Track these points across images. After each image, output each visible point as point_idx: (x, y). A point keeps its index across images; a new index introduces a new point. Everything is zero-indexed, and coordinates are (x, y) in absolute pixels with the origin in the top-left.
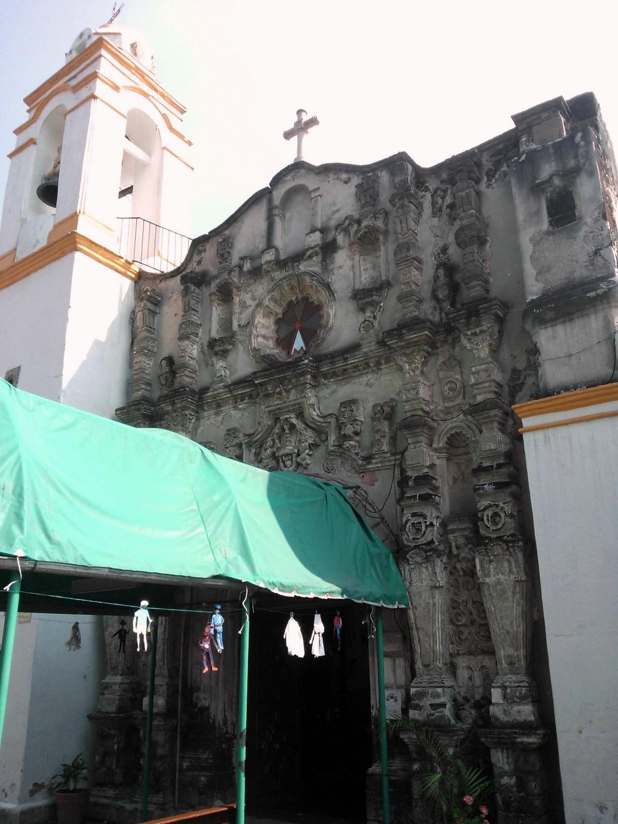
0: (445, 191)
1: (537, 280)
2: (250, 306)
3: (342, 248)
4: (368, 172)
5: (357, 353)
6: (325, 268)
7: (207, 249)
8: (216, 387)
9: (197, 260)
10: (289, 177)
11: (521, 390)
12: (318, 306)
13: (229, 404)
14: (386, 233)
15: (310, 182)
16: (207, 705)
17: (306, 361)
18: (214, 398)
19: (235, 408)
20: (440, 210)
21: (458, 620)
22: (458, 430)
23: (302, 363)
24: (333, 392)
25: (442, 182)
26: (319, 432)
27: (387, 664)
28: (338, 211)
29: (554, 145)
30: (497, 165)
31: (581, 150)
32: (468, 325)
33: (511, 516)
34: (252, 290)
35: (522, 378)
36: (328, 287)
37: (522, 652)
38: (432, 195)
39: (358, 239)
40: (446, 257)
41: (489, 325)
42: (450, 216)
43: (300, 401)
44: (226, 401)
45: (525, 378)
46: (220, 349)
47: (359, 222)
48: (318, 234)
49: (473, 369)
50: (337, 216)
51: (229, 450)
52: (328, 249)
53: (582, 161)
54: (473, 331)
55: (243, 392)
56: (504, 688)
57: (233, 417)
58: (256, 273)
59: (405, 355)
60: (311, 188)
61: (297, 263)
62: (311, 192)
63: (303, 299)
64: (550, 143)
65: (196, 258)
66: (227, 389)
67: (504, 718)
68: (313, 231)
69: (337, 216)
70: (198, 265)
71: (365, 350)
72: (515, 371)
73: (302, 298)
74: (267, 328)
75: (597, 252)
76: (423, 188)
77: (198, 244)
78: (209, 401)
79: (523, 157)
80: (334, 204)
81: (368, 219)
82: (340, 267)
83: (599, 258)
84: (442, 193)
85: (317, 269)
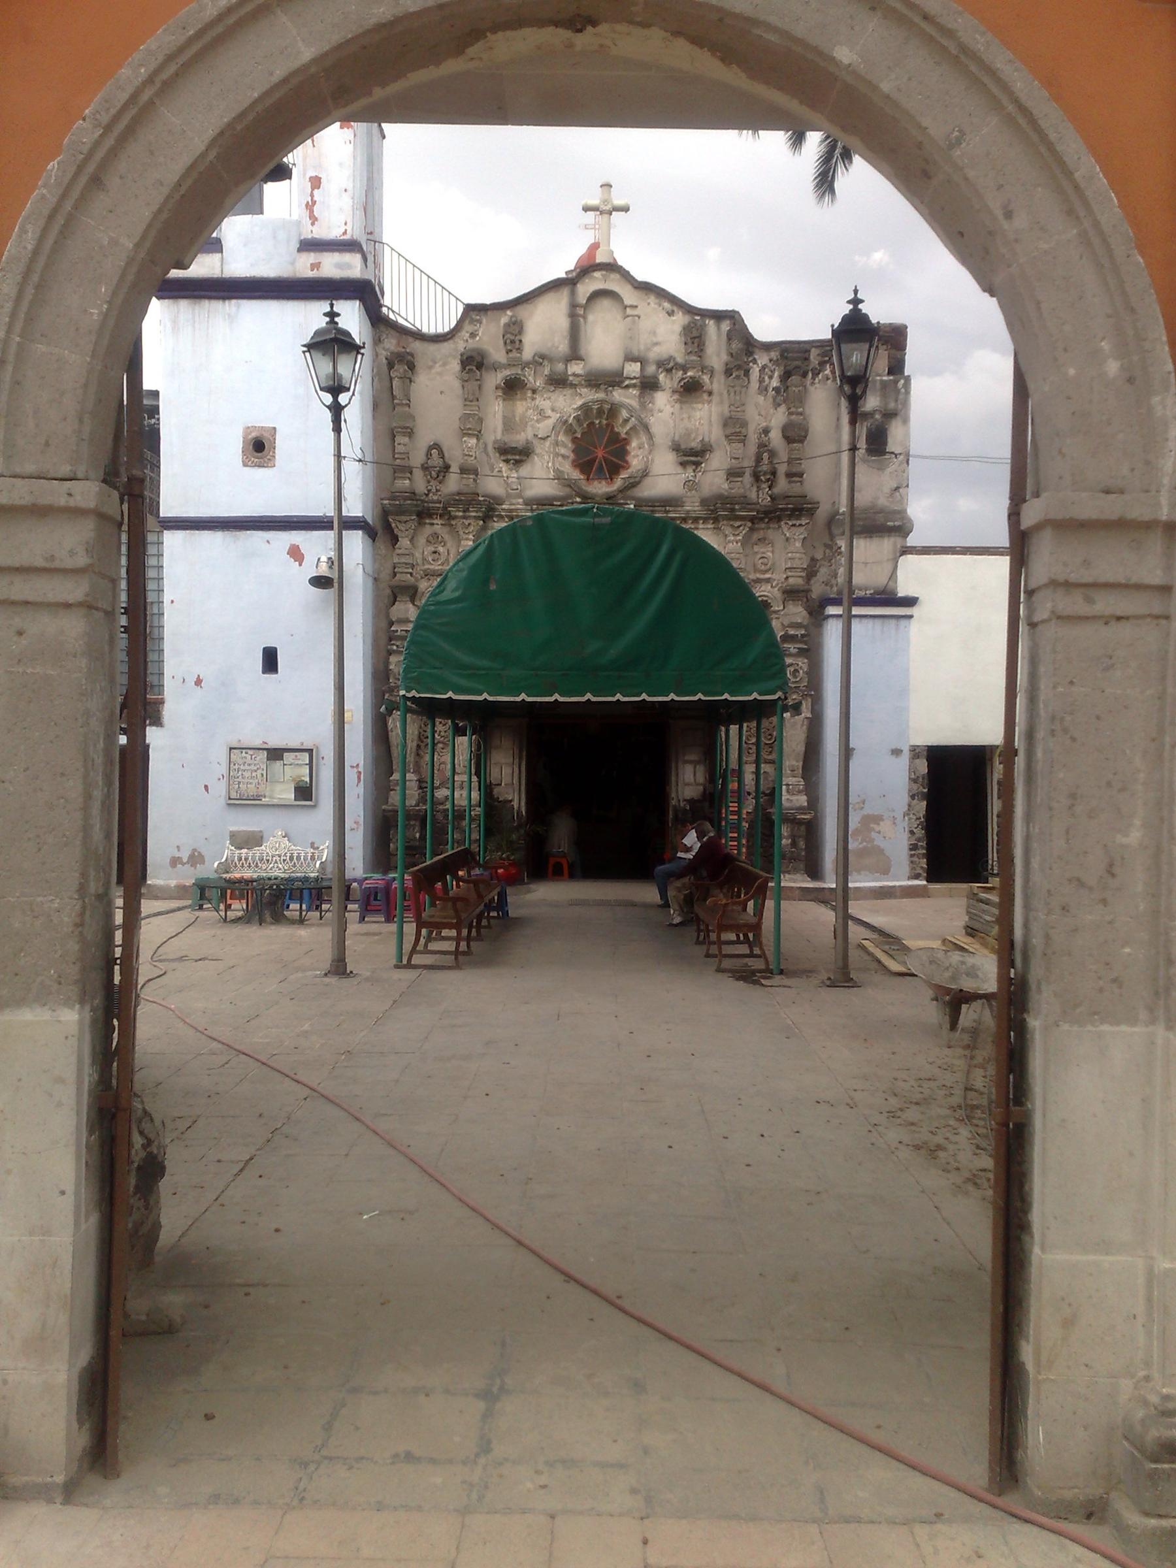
0: (773, 371)
2: (549, 417)
3: (663, 390)
4: (698, 315)
5: (679, 509)
6: (643, 405)
7: (484, 321)
8: (514, 501)
9: (471, 332)
10: (597, 274)
11: (816, 576)
12: (625, 439)
14: (710, 393)
15: (629, 295)
16: (510, 799)
17: (632, 506)
20: (766, 389)
21: (748, 740)
22: (765, 599)
28: (656, 344)
29: (882, 381)
30: (822, 364)
31: (901, 397)
32: (790, 517)
33: (807, 673)
34: (550, 398)
35: (818, 566)
36: (646, 428)
37: (801, 764)
38: (760, 370)
39: (681, 386)
40: (767, 438)
41: (808, 521)
42: (774, 399)
45: (820, 567)
46: (514, 457)
47: (685, 369)
48: (639, 364)
49: (790, 555)
50: (657, 349)
52: (648, 385)
53: (900, 406)
54: (794, 522)
58: (559, 382)
60: (627, 302)
61: (610, 388)
62: (626, 307)
63: (607, 425)
64: (878, 378)
65: (468, 328)
66: (529, 508)
68: (630, 358)
69: (657, 349)
70: (470, 337)
71: (688, 508)
72: (813, 559)
73: (606, 424)
74: (565, 446)
75: (897, 489)
76: (750, 359)
77: (473, 311)
80: (654, 333)
81: (695, 370)
82: (660, 411)
83: (898, 494)
84: (770, 373)
85: (634, 403)
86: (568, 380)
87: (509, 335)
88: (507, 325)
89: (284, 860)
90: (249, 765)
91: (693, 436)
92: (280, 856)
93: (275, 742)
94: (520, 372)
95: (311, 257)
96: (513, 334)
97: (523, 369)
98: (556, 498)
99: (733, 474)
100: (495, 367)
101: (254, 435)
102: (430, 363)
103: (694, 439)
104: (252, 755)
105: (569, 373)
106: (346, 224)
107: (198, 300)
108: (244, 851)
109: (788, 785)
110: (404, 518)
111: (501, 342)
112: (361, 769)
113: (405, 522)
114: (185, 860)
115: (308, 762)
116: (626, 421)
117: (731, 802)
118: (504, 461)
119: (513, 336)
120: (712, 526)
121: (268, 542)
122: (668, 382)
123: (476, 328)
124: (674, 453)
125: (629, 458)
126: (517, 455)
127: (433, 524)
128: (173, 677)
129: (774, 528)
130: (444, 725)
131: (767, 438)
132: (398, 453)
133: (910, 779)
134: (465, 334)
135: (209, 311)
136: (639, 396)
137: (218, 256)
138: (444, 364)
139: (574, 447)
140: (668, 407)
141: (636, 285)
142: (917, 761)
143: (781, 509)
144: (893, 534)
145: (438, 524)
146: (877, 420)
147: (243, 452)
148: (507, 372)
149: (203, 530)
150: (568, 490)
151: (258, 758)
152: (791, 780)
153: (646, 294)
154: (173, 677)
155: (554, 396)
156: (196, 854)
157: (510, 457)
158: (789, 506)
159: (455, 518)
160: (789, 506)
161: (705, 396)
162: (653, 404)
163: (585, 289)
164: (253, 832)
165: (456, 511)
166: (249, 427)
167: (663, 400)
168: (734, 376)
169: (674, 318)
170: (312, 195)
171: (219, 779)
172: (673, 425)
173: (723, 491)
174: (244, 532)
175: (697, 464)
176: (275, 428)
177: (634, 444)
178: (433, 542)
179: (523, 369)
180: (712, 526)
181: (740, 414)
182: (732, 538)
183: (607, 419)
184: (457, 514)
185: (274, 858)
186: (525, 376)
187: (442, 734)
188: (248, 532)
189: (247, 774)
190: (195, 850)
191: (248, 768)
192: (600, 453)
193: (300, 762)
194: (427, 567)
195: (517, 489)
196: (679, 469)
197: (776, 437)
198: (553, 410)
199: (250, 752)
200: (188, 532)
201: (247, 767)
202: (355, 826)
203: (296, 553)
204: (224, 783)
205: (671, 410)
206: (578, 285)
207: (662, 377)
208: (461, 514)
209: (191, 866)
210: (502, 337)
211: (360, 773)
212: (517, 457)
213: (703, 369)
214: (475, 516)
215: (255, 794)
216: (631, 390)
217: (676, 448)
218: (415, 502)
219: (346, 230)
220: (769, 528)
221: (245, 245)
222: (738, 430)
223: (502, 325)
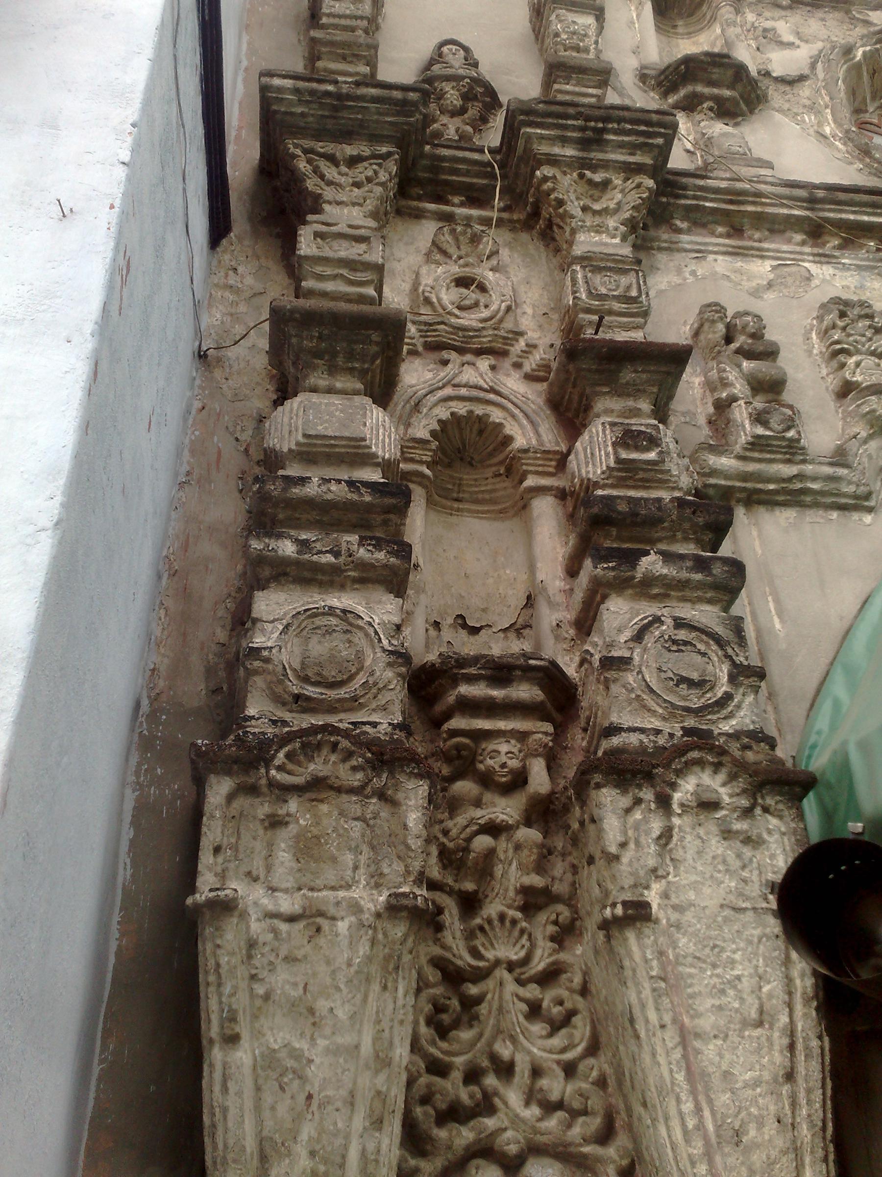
18: (731, 202)
19: (824, 258)
46: (716, 91)
51: (858, 364)
55: (866, 218)
57: (815, 282)
78: (707, 204)
110: (350, 150)
113: (353, 161)
130: (556, 1026)
132: (329, 15)
165: (552, 140)
178: (452, 250)
184: (557, 150)
208: (570, 152)
212: (727, 93)
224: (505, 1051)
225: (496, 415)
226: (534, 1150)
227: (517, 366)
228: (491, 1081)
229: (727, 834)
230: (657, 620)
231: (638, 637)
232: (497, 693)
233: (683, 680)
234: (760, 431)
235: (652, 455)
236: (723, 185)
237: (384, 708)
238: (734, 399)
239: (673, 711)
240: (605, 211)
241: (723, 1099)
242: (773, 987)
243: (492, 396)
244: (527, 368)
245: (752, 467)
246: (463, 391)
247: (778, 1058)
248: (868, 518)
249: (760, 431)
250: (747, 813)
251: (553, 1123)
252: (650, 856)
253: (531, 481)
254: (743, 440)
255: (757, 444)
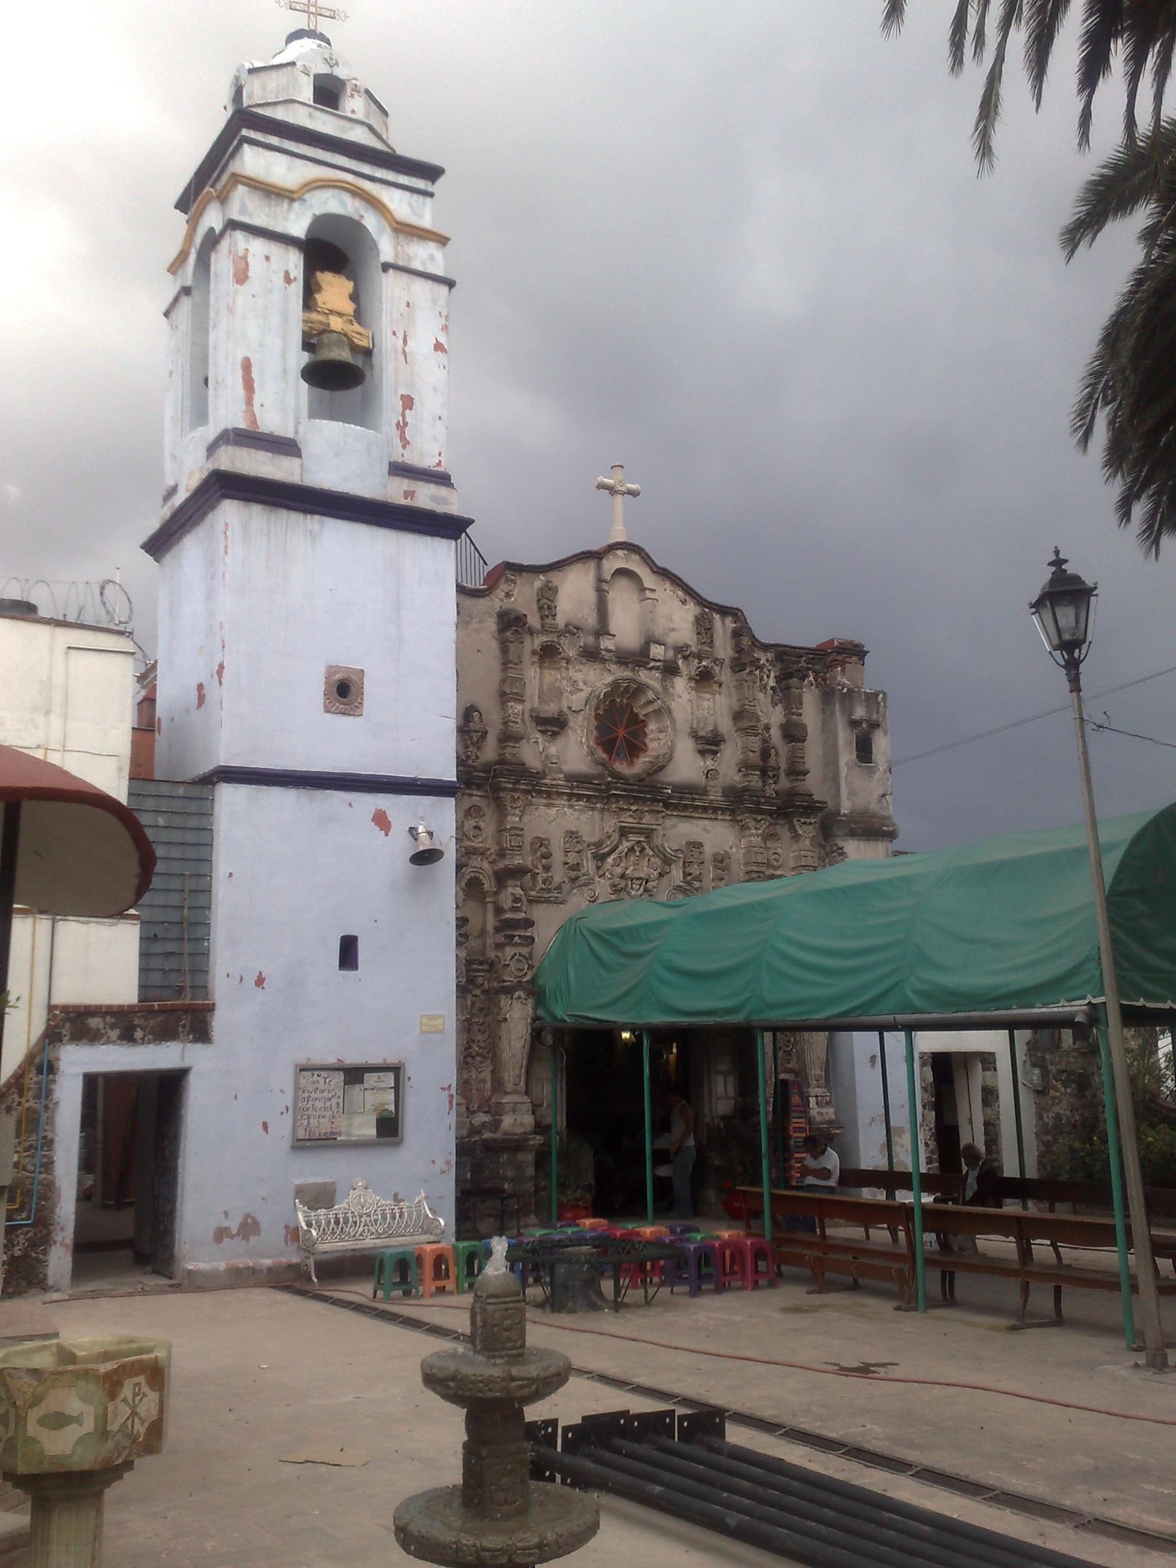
0: (769, 671)
1: (848, 799)
5: (705, 797)
7: (518, 582)
8: (556, 776)
10: (620, 553)
12: (643, 721)
13: (562, 799)
17: (670, 791)
19: (571, 806)
23: (665, 791)
24: (674, 826)
25: (767, 660)
26: (667, 861)
27: (720, 1080)
29: (865, 692)
31: (881, 709)
32: (802, 815)
36: (670, 712)
39: (697, 675)
40: (767, 735)
43: (655, 827)
44: (560, 794)
46: (553, 729)
47: (699, 656)
52: (670, 670)
53: (881, 719)
55: (585, 793)
56: (816, 1096)
58: (591, 655)
59: (755, 819)
61: (637, 668)
63: (627, 705)
65: (503, 587)
66: (569, 785)
67: (818, 1118)
69: (673, 634)
77: (512, 569)
79: (845, 690)
80: (671, 620)
84: (767, 672)
85: (656, 685)
86: (600, 654)
87: (545, 601)
88: (541, 590)
89: (376, 1221)
90: (322, 1092)
91: (702, 724)
92: (369, 1216)
93: (353, 1058)
94: (556, 640)
95: (404, 484)
96: (549, 600)
97: (558, 637)
98: (595, 777)
99: (745, 766)
100: (531, 632)
101: (338, 676)
102: (467, 619)
103: (703, 728)
104: (325, 1078)
105: (602, 647)
106: (440, 454)
107: (274, 508)
108: (322, 1211)
109: (816, 1096)
111: (535, 606)
112: (453, 1091)
114: (234, 1231)
115: (393, 1085)
116: (651, 702)
117: (795, 1118)
118: (540, 731)
119: (546, 600)
120: (729, 818)
121: (350, 805)
122: (685, 668)
123: (511, 588)
124: (694, 740)
125: (647, 741)
126: (553, 725)
127: (471, 795)
128: (228, 975)
129: (781, 825)
130: (483, 1033)
131: (767, 735)
133: (922, 1087)
134: (500, 592)
135: (287, 525)
136: (662, 678)
137: (297, 461)
138: (481, 621)
139: (596, 724)
140: (686, 693)
141: (655, 570)
142: (925, 1069)
143: (798, 805)
144: (885, 839)
145: (476, 796)
146: (863, 729)
147: (325, 694)
148: (544, 638)
149: (274, 785)
150: (600, 768)
151: (332, 1083)
152: (819, 1091)
153: (663, 580)
154: (228, 975)
155: (585, 669)
156: (249, 1221)
157: (549, 728)
158: (805, 803)
159: (505, 789)
160: (805, 803)
161: (716, 687)
162: (673, 688)
163: (611, 564)
164: (325, 1184)
165: (506, 782)
166: (331, 667)
167: (680, 685)
168: (748, 670)
169: (687, 607)
170: (404, 416)
171: (282, 1113)
172: (689, 710)
173: (735, 783)
174: (323, 791)
175: (715, 753)
176: (363, 671)
177: (652, 726)
179: (558, 637)
180: (729, 818)
181: (753, 708)
182: (754, 832)
183: (627, 699)
184: (507, 785)
185: (363, 1220)
186: (560, 644)
187: (482, 1044)
188: (328, 791)
189: (319, 1104)
190: (248, 1215)
191: (321, 1095)
192: (621, 732)
193: (383, 1085)
194: (467, 843)
195: (556, 763)
196: (698, 757)
197: (775, 734)
198: (585, 683)
199: (324, 1074)
200: (253, 786)
201: (318, 1095)
202: (445, 1168)
203: (382, 821)
204: (288, 1119)
205: (688, 697)
206: (604, 561)
207: (680, 662)
208: (511, 786)
209: (243, 1238)
210: (536, 599)
211: (452, 1096)
212: (556, 729)
213: (715, 661)
214: (524, 790)
215: (329, 1130)
216: (654, 672)
217: (695, 735)
218: (467, 769)
219: (440, 461)
220: (777, 824)
221: (336, 456)
222: (754, 724)
223: (536, 588)
224: (474, 1038)
225: (481, 877)
226: (477, 1055)
227: (487, 858)
228: (471, 1043)
229: (522, 1003)
230: (516, 955)
231: (512, 959)
232: (480, 967)
233: (519, 969)
234: (544, 887)
235: (519, 905)
236: (548, 781)
237: (463, 977)
238: (538, 874)
239: (516, 977)
240: (517, 807)
241: (513, 1050)
242: (525, 1031)
243: (480, 870)
244: (490, 860)
245: (540, 895)
246: (475, 870)
247: (523, 1044)
248: (562, 906)
249: (544, 887)
250: (526, 999)
251: (480, 1050)
252: (508, 1008)
253: (488, 899)
254: (538, 888)
255: (542, 889)
